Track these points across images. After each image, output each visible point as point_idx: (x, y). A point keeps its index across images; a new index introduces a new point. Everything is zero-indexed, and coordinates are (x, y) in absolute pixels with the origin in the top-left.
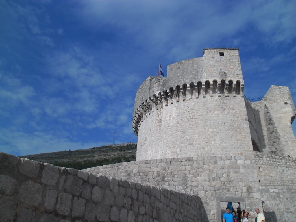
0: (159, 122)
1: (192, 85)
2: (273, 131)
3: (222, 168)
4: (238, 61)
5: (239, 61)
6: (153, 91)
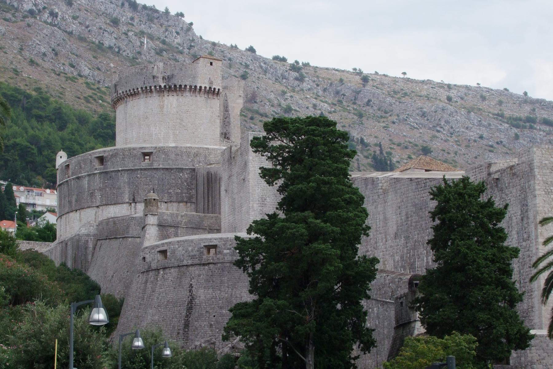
0: (162, 107)
1: (191, 87)
6: (158, 81)
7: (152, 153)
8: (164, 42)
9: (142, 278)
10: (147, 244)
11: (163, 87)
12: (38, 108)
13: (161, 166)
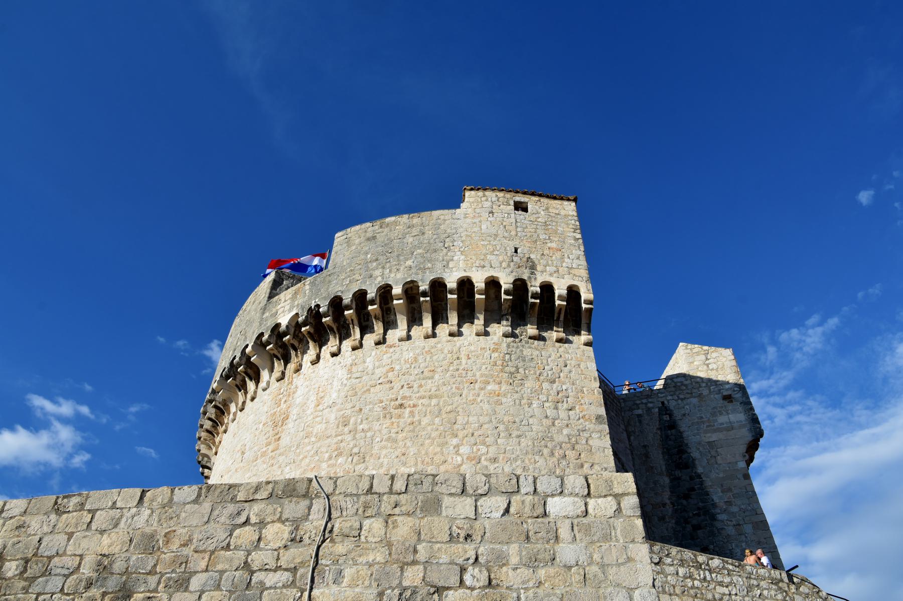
2: (693, 489)
3: (462, 535)
4: (574, 232)
5: (579, 231)
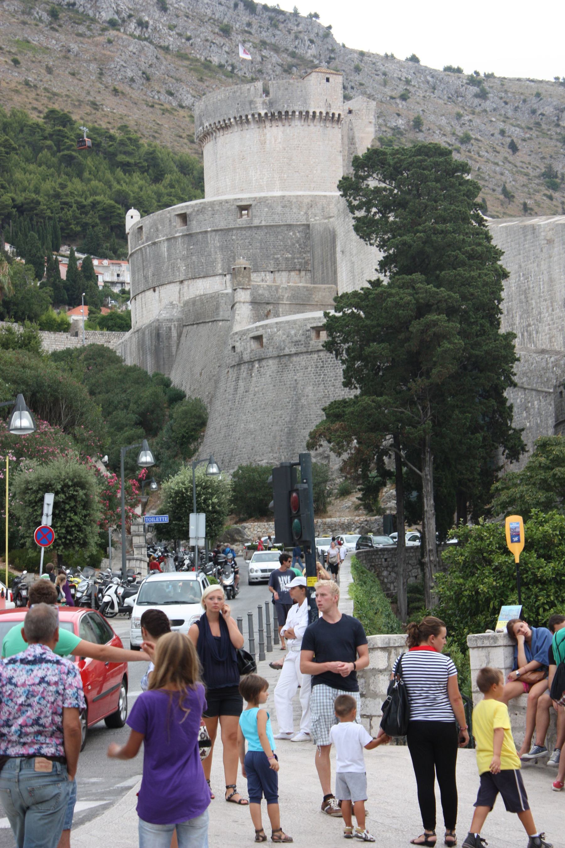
0: (263, 143)
1: (301, 113)
6: (256, 108)
7: (250, 205)
8: (293, 55)
9: (233, 374)
10: (237, 328)
11: (263, 114)
12: (125, 153)
13: (263, 223)
